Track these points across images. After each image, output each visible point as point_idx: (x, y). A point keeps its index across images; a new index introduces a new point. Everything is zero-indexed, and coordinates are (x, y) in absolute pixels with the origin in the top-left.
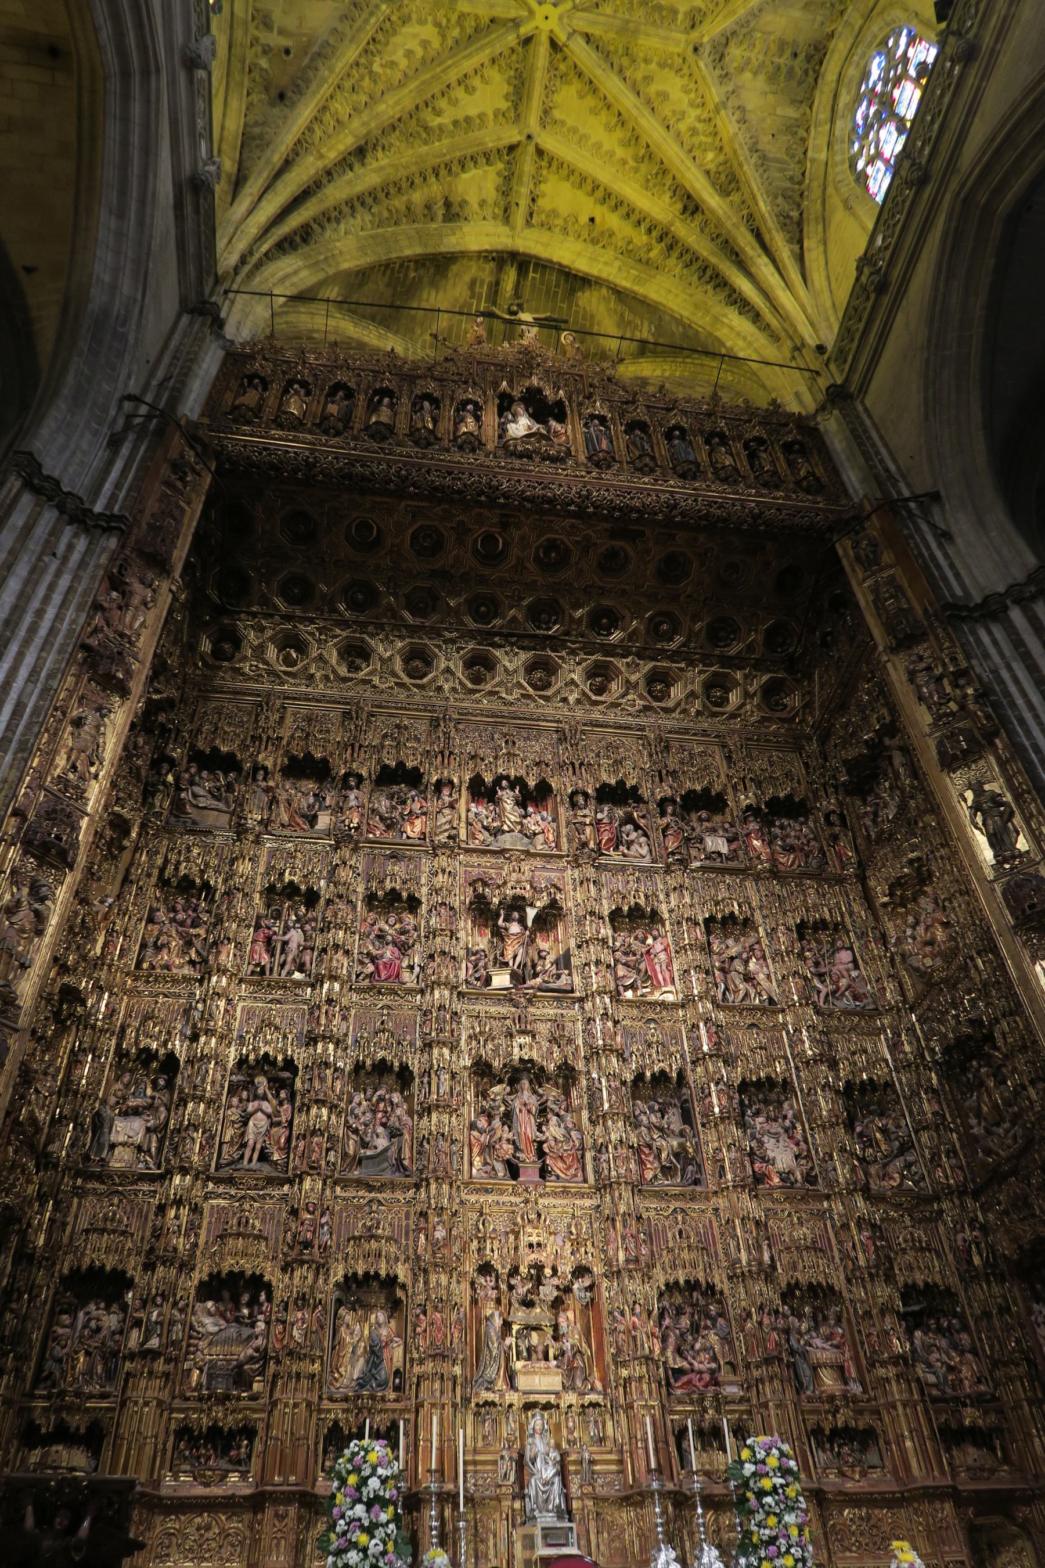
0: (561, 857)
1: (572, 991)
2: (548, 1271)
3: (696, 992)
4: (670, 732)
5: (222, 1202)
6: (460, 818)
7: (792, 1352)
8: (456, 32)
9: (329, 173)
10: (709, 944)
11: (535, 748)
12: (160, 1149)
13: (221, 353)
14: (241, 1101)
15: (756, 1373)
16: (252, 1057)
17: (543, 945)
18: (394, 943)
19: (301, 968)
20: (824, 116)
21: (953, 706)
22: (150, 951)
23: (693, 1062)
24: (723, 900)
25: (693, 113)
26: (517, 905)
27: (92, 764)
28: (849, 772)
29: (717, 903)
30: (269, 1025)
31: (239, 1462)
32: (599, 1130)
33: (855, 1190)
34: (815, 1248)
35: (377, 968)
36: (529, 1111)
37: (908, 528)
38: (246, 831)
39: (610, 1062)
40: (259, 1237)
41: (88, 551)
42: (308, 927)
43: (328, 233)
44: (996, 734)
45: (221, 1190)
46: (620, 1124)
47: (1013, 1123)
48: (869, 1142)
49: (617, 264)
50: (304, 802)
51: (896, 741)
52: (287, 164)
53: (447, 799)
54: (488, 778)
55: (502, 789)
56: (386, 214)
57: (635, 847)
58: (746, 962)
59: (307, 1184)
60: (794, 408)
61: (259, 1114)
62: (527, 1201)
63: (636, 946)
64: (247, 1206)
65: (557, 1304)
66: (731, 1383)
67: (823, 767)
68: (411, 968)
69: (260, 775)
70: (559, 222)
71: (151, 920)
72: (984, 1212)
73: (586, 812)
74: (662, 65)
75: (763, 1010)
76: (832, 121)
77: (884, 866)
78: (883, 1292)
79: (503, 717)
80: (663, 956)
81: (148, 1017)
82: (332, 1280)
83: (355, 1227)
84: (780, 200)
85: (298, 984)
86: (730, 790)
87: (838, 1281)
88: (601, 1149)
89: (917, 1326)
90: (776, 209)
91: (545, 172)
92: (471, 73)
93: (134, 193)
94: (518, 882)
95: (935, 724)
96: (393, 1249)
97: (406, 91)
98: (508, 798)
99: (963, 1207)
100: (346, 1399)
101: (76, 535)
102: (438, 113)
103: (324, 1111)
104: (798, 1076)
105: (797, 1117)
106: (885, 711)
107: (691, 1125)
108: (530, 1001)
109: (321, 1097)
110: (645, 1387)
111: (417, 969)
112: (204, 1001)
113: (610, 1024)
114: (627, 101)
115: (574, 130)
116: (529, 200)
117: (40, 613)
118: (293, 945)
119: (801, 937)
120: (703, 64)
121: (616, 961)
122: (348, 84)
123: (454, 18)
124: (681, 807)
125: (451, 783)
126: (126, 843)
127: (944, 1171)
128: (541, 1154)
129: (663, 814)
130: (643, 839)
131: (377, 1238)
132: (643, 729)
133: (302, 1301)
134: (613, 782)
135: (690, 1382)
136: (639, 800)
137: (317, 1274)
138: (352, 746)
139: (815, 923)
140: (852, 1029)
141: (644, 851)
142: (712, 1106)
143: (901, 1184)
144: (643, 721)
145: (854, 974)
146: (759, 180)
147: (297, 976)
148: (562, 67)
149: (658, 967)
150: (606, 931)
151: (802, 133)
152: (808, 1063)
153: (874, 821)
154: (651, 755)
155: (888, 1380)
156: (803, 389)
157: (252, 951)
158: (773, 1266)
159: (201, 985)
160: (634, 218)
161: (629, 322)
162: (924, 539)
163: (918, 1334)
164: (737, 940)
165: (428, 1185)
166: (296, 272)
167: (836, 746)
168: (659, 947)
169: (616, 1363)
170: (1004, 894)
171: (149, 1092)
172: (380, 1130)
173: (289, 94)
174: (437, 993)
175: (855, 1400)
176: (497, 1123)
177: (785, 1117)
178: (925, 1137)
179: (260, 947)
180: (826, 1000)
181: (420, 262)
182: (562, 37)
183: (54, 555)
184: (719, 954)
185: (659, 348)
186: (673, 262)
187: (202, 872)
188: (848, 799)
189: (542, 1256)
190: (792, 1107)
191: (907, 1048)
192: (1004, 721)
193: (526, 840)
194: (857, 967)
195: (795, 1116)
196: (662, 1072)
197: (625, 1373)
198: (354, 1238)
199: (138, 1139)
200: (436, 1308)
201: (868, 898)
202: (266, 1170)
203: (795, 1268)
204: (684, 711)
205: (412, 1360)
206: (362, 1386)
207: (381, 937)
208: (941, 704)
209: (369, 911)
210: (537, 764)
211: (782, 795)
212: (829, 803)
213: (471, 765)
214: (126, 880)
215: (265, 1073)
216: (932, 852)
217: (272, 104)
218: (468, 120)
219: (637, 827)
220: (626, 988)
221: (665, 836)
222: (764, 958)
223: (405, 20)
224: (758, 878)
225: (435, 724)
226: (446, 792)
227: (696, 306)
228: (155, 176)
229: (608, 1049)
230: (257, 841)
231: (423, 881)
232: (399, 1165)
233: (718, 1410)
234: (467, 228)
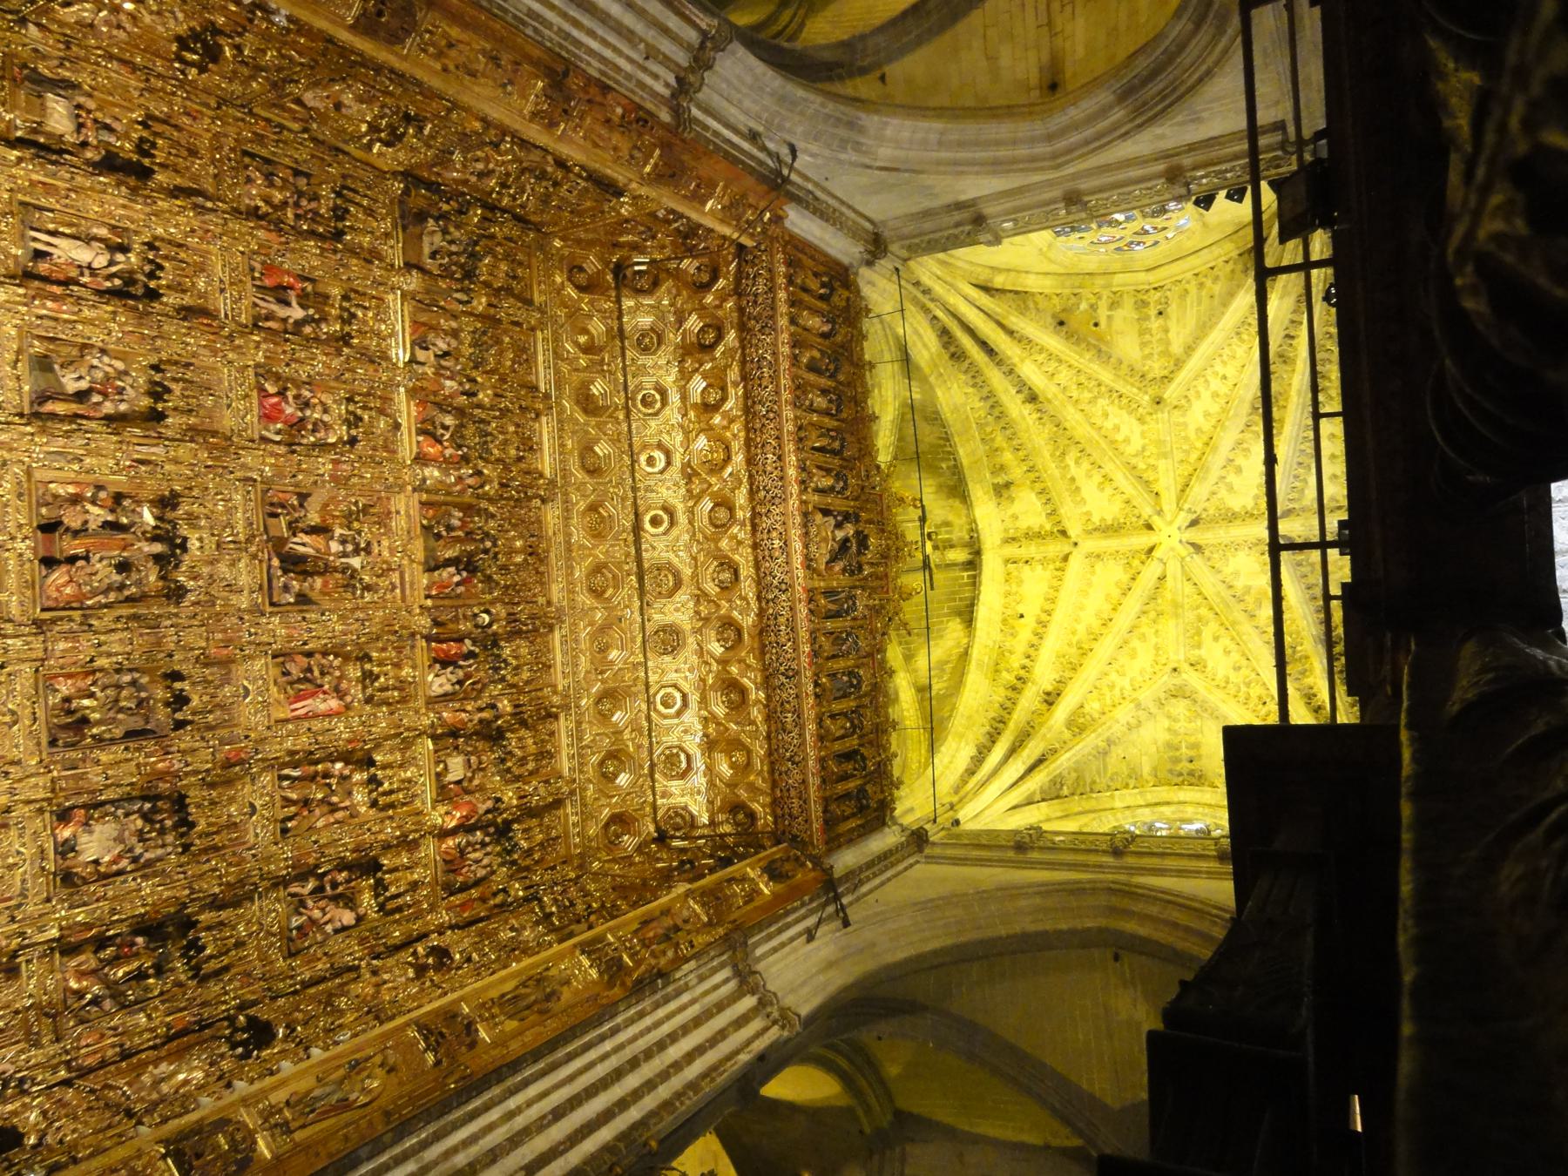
8: (1142, 466)
9: (1011, 372)
13: (846, 260)
20: (1150, 798)
25: (1126, 683)
37: (811, 901)
41: (654, 94)
43: (963, 377)
49: (990, 643)
52: (1010, 333)
56: (989, 429)
60: (899, 809)
70: (1014, 588)
74: (1157, 648)
76: (1148, 805)
84: (1074, 775)
90: (1065, 773)
91: (1051, 567)
92: (1115, 485)
93: (963, 155)
97: (1089, 428)
101: (667, 85)
102: (1077, 463)
114: (1123, 621)
115: (1090, 584)
116: (1026, 557)
117: (591, 33)
120: (1166, 680)
122: (1082, 379)
123: (1152, 461)
128: (72, 560)
146: (1086, 751)
148: (1136, 563)
151: (1132, 783)
156: (918, 814)
160: (1031, 651)
161: (943, 670)
162: (804, 917)
166: (925, 345)
173: (1064, 329)
181: (957, 471)
182: (1157, 554)
183: (647, 58)
185: (927, 704)
186: (1000, 695)
194: (336, 931)
217: (1054, 316)
218: (1078, 489)
223: (1141, 420)
227: (969, 718)
228: (977, 173)
234: (992, 505)
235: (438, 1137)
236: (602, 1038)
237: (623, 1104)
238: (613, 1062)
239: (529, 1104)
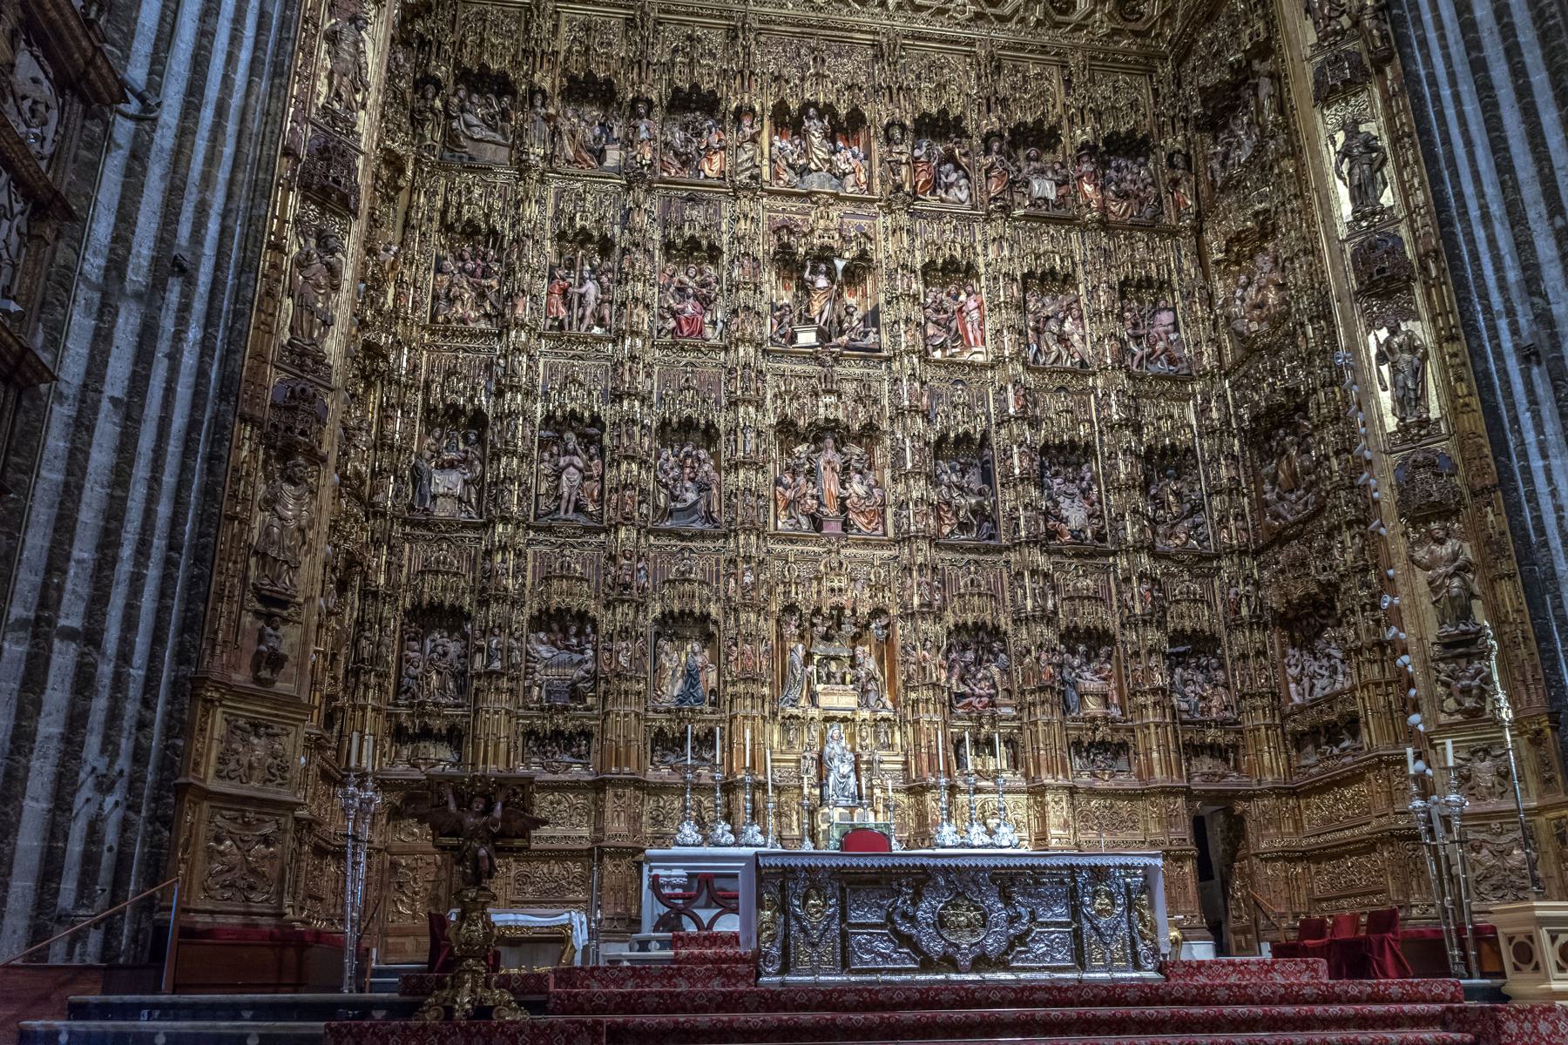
0: (873, 201)
1: (880, 350)
2: (848, 612)
3: (1007, 353)
4: (1003, 48)
5: (545, 549)
6: (762, 153)
7: (1063, 682)
10: (1025, 302)
11: (847, 68)
12: (479, 500)
14: (552, 455)
15: (1029, 698)
16: (559, 413)
17: (850, 300)
18: (696, 297)
19: (600, 322)
21: (1345, 21)
22: (443, 304)
23: (998, 425)
24: (1045, 253)
26: (824, 256)
27: (357, 91)
28: (1204, 104)
29: (1038, 257)
30: (574, 381)
31: (580, 757)
32: (901, 487)
33: (1142, 548)
34: (1095, 598)
35: (679, 323)
36: (833, 469)
38: (529, 168)
39: (914, 422)
40: (580, 579)
42: (604, 279)
44: (1389, 59)
45: (541, 538)
46: (922, 483)
47: (1307, 491)
48: (1161, 503)
50: (590, 133)
51: (1267, 66)
53: (748, 131)
54: (794, 105)
55: (809, 118)
57: (954, 190)
58: (1062, 322)
59: (622, 534)
61: (571, 469)
62: (830, 552)
63: (949, 303)
64: (567, 552)
65: (856, 638)
66: (1006, 705)
67: (1175, 95)
68: (714, 323)
69: (538, 102)
71: (439, 270)
72: (1261, 568)
73: (902, 148)
75: (1074, 373)
77: (1225, 218)
78: (1153, 636)
79: (811, 26)
80: (975, 314)
81: (450, 373)
82: (651, 616)
83: (669, 571)
85: (598, 339)
86: (1065, 123)
87: (1113, 624)
88: (902, 505)
89: (1178, 664)
94: (826, 230)
95: (1318, 46)
96: (706, 591)
98: (815, 130)
99: (1241, 566)
100: (669, 711)
103: (634, 467)
104: (1101, 440)
105: (1094, 479)
106: (1260, 25)
107: (990, 485)
108: (836, 360)
109: (630, 453)
110: (931, 707)
111: (720, 325)
112: (505, 357)
113: (917, 385)
118: (591, 298)
119: (1123, 296)
121: (927, 318)
124: (1009, 143)
125: (752, 110)
126: (401, 182)
127: (1230, 533)
129: (988, 151)
130: (963, 182)
131: (690, 581)
132: (972, 44)
133: (625, 633)
134: (934, 110)
135: (970, 703)
136: (963, 134)
137: (637, 611)
138: (638, 63)
139: (1140, 280)
140: (1163, 394)
141: (963, 196)
142: (1012, 466)
143: (1186, 543)
144: (973, 33)
145: (1173, 337)
147: (597, 330)
149: (969, 326)
150: (917, 286)
152: (1112, 427)
153: (1223, 165)
154: (979, 78)
155: (1145, 706)
157: (549, 304)
158: (1055, 613)
159: (500, 340)
163: (1179, 670)
164: (1054, 298)
165: (737, 535)
167: (1194, 69)
168: (972, 304)
169: (906, 689)
170: (1353, 255)
171: (461, 446)
172: (688, 484)
174: (741, 350)
175: (1114, 720)
176: (801, 480)
177: (1082, 479)
178: (1216, 501)
179: (556, 299)
180: (1140, 365)
184: (1035, 313)
187: (487, 216)
188: (1197, 136)
189: (843, 600)
190: (1090, 469)
191: (1215, 415)
192: (1402, 41)
193: (835, 181)
195: (1092, 478)
196: (966, 433)
197: (913, 695)
198: (669, 581)
199: (458, 490)
200: (746, 641)
201: (1200, 255)
202: (582, 520)
203: (1075, 614)
204: (1022, 20)
205: (725, 682)
206: (681, 702)
207: (681, 290)
208: (1331, 18)
209: (668, 261)
210: (850, 88)
211: (1123, 130)
212: (1174, 142)
213: (774, 89)
214: (407, 225)
215: (573, 429)
216: (1283, 204)
219: (958, 167)
220: (935, 348)
221: (988, 178)
222: (1081, 318)
224: (1084, 228)
225: (732, 34)
226: (747, 122)
229: (914, 410)
230: (542, 181)
231: (724, 227)
232: (709, 517)
233: (993, 726)
235: (1484, 296)
236: (1437, 98)
237: (1524, 92)
238: (1467, 88)
239: (1481, 195)
